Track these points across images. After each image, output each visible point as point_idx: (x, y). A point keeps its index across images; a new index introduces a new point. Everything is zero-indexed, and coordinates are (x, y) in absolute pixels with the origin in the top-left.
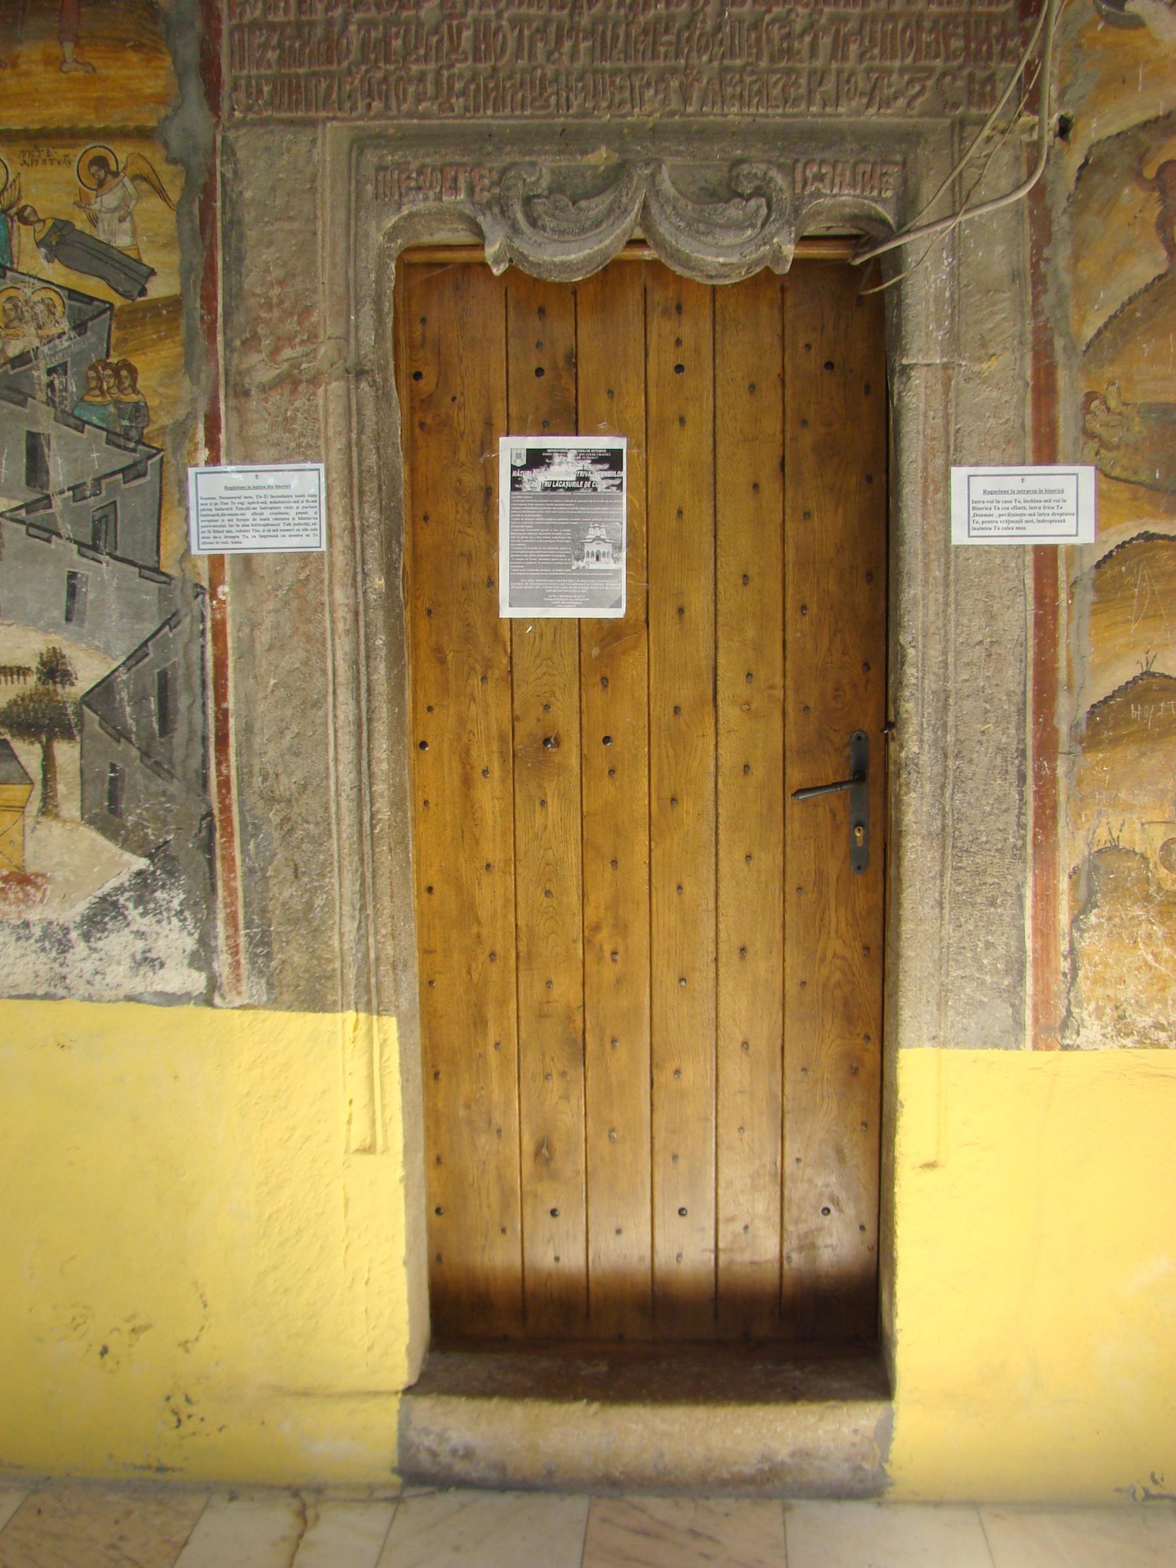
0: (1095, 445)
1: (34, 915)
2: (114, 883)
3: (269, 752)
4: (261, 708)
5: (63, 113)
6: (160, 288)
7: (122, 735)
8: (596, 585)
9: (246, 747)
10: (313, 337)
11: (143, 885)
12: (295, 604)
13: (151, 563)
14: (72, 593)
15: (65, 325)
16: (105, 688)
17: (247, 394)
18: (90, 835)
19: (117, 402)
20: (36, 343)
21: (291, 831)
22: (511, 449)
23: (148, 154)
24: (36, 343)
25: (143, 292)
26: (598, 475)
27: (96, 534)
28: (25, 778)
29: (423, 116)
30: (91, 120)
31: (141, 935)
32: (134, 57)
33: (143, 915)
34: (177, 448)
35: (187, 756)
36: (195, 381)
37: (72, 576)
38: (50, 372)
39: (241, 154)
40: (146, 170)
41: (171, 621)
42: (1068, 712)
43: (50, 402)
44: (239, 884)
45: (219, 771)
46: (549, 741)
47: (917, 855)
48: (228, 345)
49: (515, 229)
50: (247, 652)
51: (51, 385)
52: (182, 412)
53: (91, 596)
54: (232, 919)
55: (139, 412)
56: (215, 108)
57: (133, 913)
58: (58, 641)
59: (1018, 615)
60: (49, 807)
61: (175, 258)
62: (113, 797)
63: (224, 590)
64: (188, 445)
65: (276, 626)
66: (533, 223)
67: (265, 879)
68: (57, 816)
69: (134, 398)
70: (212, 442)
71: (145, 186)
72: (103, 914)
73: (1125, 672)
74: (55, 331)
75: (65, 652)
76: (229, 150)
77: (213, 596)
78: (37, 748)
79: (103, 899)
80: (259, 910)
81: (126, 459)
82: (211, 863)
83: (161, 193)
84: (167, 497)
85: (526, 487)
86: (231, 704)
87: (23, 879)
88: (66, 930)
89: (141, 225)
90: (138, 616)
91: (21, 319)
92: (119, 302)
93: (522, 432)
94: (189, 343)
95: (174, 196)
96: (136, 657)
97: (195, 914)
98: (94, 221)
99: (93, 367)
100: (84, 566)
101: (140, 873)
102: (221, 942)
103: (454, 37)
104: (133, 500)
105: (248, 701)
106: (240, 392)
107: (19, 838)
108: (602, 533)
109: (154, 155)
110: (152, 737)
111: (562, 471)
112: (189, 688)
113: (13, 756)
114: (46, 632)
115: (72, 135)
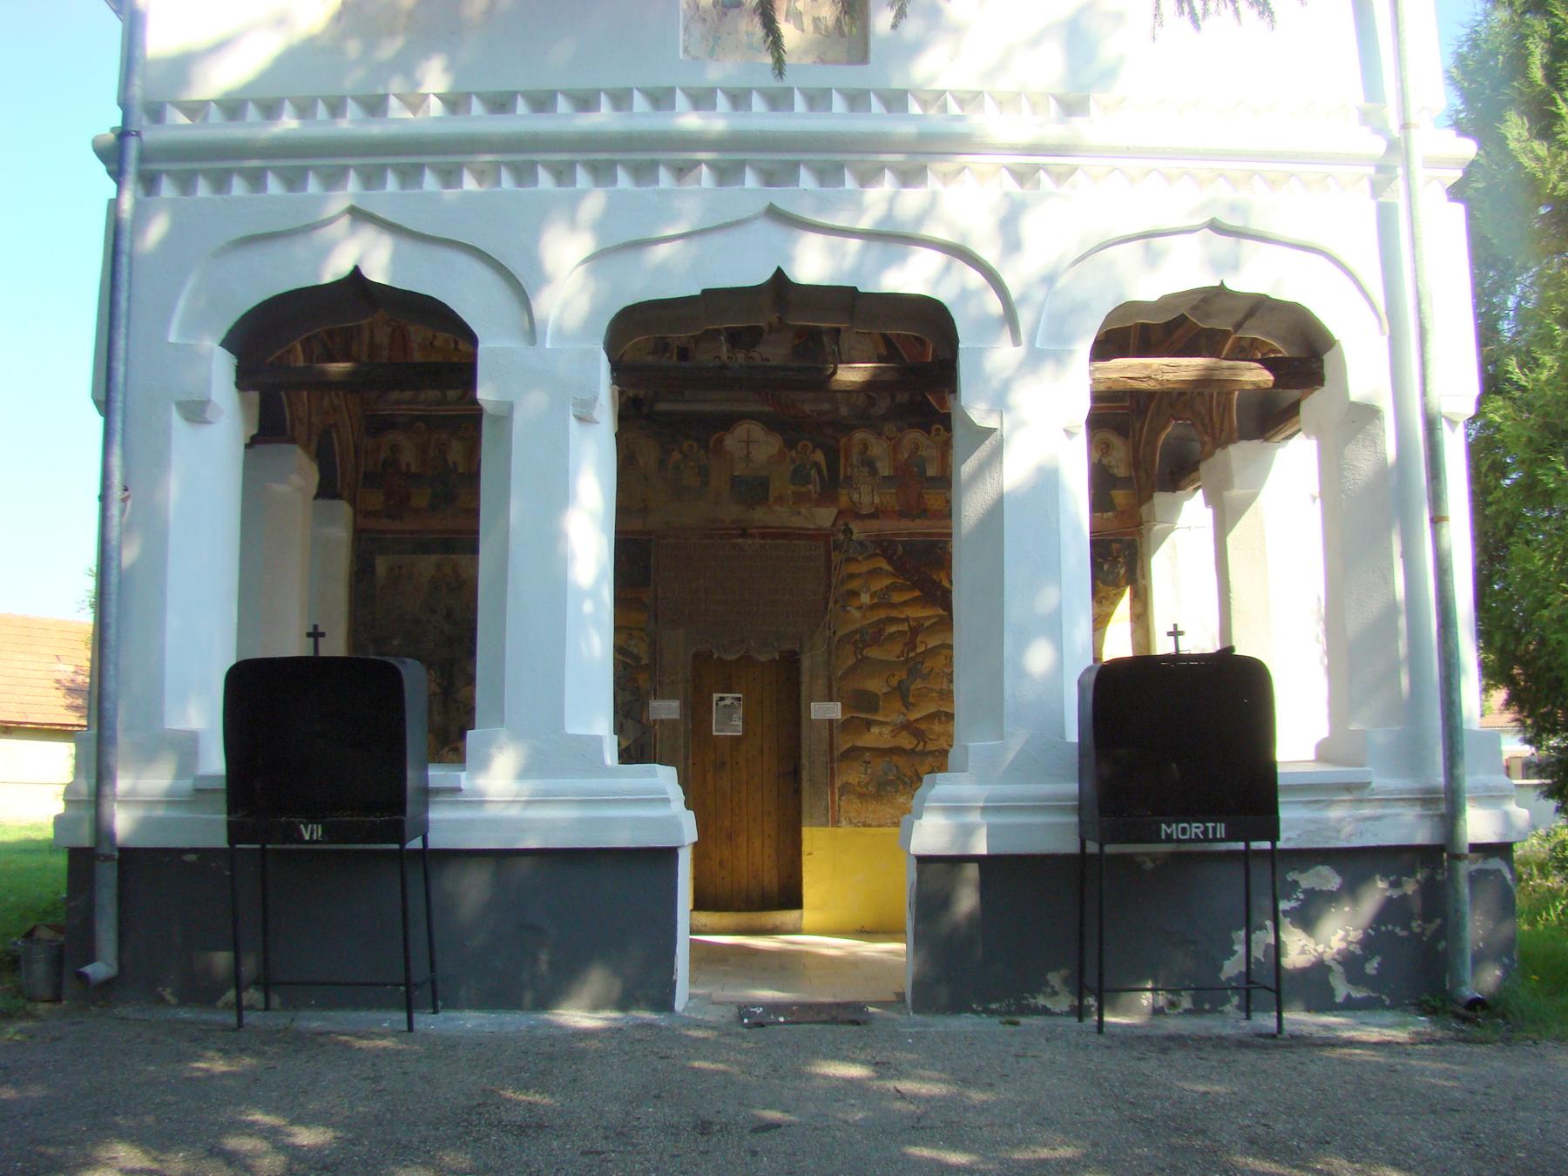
0: (840, 698)
6: (644, 661)
22: (716, 696)
42: (836, 754)
46: (724, 763)
47: (805, 785)
55: (638, 688)
59: (826, 733)
73: (849, 745)
84: (645, 706)
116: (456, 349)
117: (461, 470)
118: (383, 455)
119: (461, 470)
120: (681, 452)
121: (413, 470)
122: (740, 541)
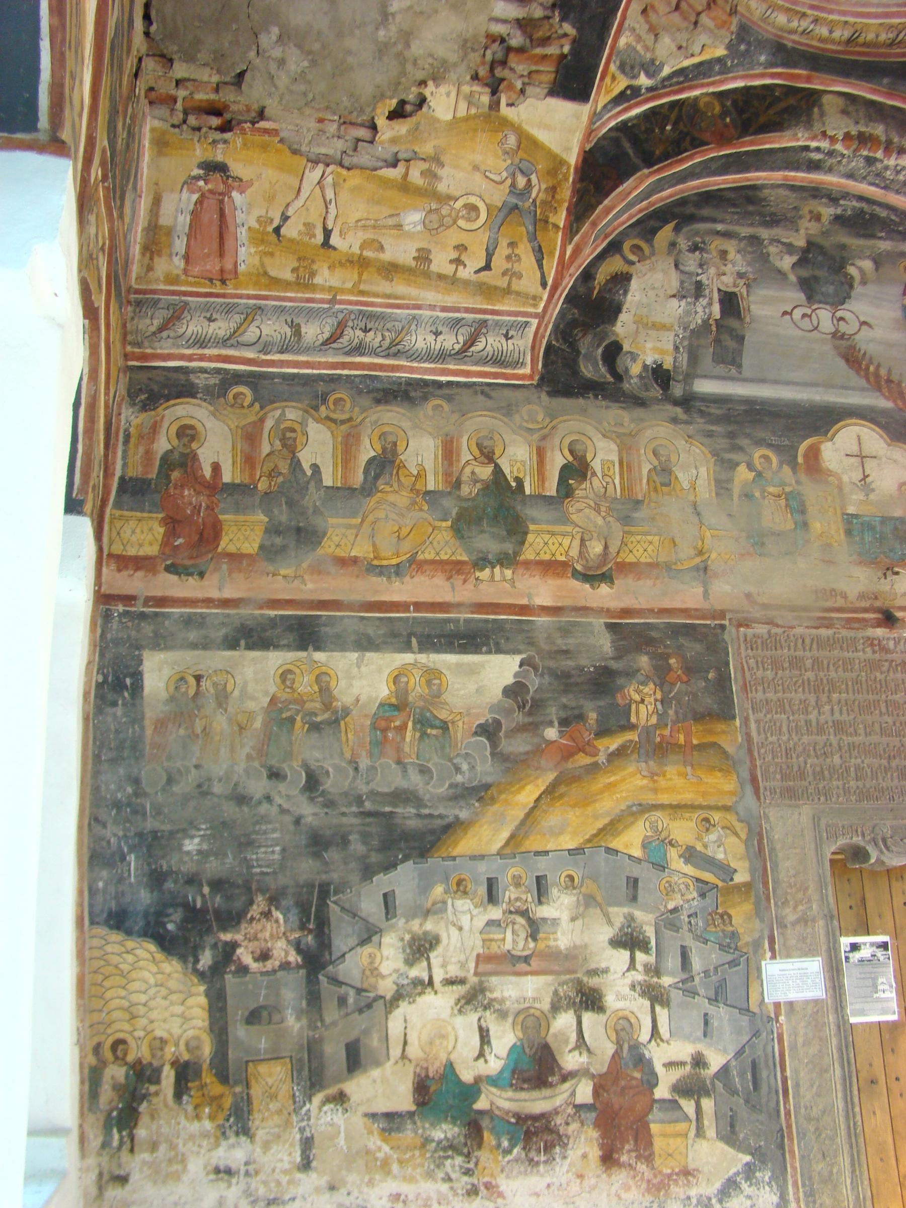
1: (693, 1192)
2: (734, 1170)
3: (807, 1095)
4: (802, 1074)
5: (687, 797)
6: (739, 878)
7: (734, 1092)
8: (885, 1005)
9: (797, 1094)
10: (810, 901)
11: (749, 1171)
12: (813, 1023)
13: (745, 1006)
14: (706, 1023)
15: (695, 894)
16: (725, 1070)
17: (786, 926)
18: (721, 1146)
19: (723, 931)
20: (681, 903)
21: (820, 1135)
23: (728, 817)
24: (681, 903)
25: (732, 879)
26: (880, 953)
27: (716, 993)
28: (687, 1118)
29: (842, 803)
30: (700, 801)
31: (749, 1197)
32: (719, 774)
33: (749, 1186)
34: (756, 952)
35: (768, 1101)
36: (762, 920)
37: (706, 1015)
38: (689, 916)
39: (771, 819)
40: (729, 825)
41: (756, 1034)
43: (690, 930)
44: (798, 1165)
45: (785, 1108)
48: (776, 904)
49: (881, 852)
50: (793, 1047)
51: (690, 922)
52: (756, 935)
53: (716, 1024)
54: (795, 1183)
55: (734, 935)
56: (759, 799)
57: (744, 1186)
58: (701, 1047)
60: (700, 1132)
61: (746, 864)
62: (732, 1126)
63: (782, 1018)
64: (761, 951)
65: (806, 1034)
66: (887, 848)
67: (810, 1160)
68: (705, 1137)
69: (731, 928)
70: (772, 949)
71: (728, 832)
72: (730, 1187)
74: (690, 897)
75: (705, 1052)
76: (767, 817)
77: (777, 1021)
78: (693, 1102)
79: (729, 1180)
80: (808, 1177)
81: (730, 957)
82: (784, 1155)
83: (736, 834)
84: (752, 974)
85: (851, 960)
86: (788, 1073)
87: (686, 1173)
88: (709, 1199)
89: (727, 848)
90: (739, 1033)
91: (673, 891)
92: (720, 884)
93: (847, 935)
94: (757, 904)
95: (744, 836)
96: (739, 1053)
97: (777, 1184)
98: (706, 846)
99: (710, 914)
100: (711, 1010)
101: (747, 1164)
102: (791, 1197)
103: (847, 770)
104: (734, 976)
105: (796, 1071)
106: (783, 926)
107: (684, 1151)
108: (884, 980)
109: (731, 818)
110: (749, 1093)
111: (865, 953)
112: (767, 1066)
113: (680, 1108)
114: (694, 1042)
115: (692, 807)
116: (326, 244)
117: (328, 481)
118: (162, 445)
119: (328, 481)
120: (750, 467)
121: (227, 478)
122: (880, 632)
